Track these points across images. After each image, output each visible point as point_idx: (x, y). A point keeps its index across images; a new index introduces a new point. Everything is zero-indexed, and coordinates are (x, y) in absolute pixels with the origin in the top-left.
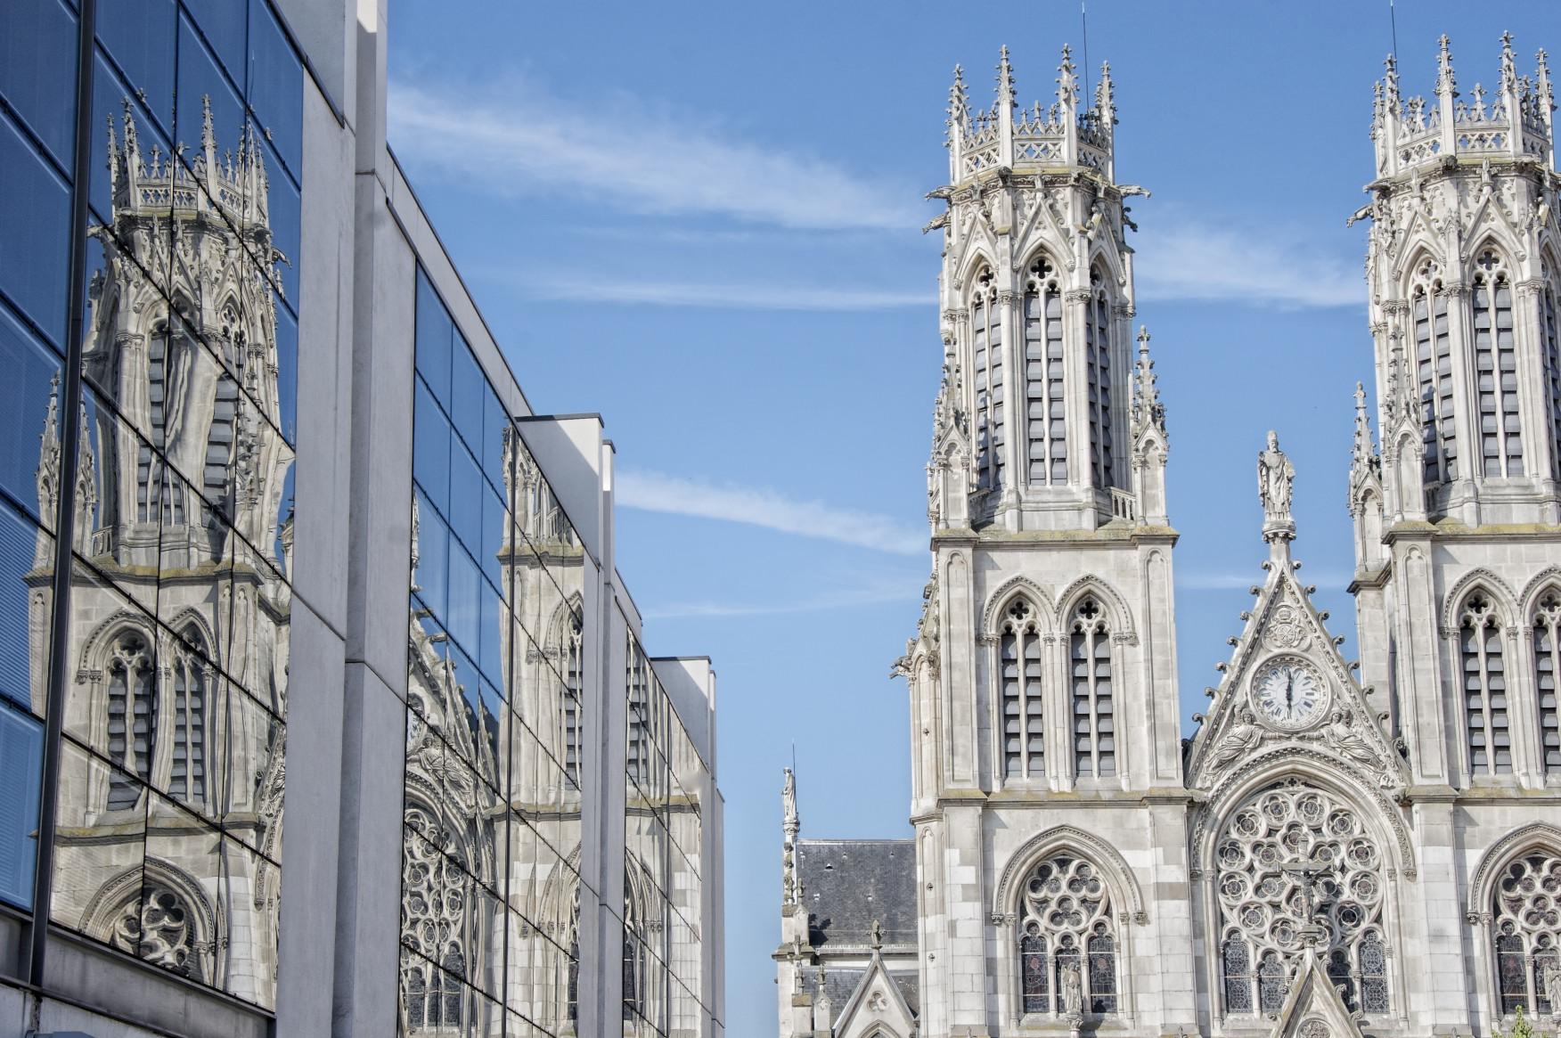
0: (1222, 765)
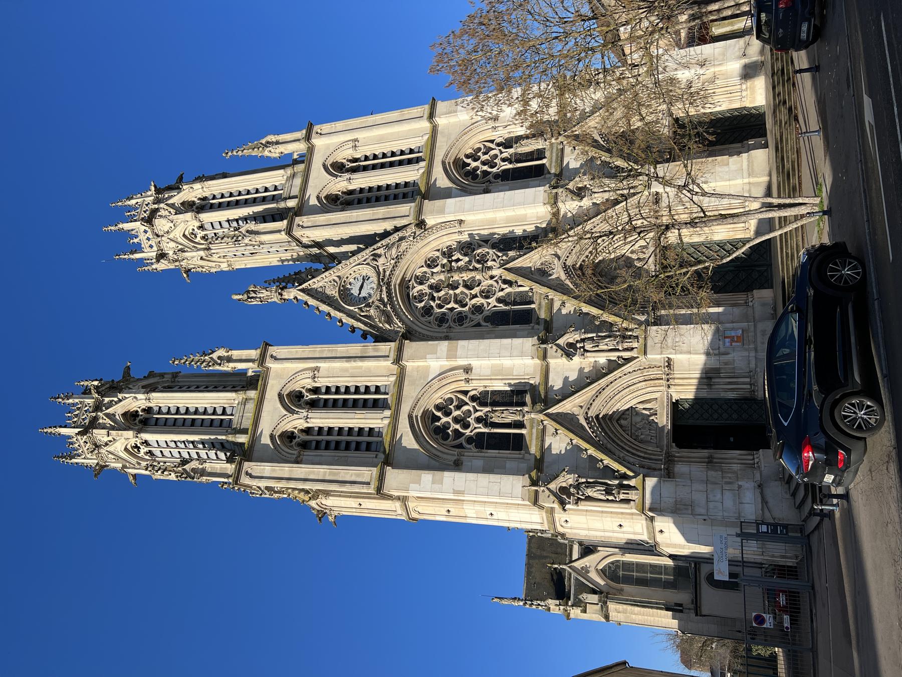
0: (389, 321)
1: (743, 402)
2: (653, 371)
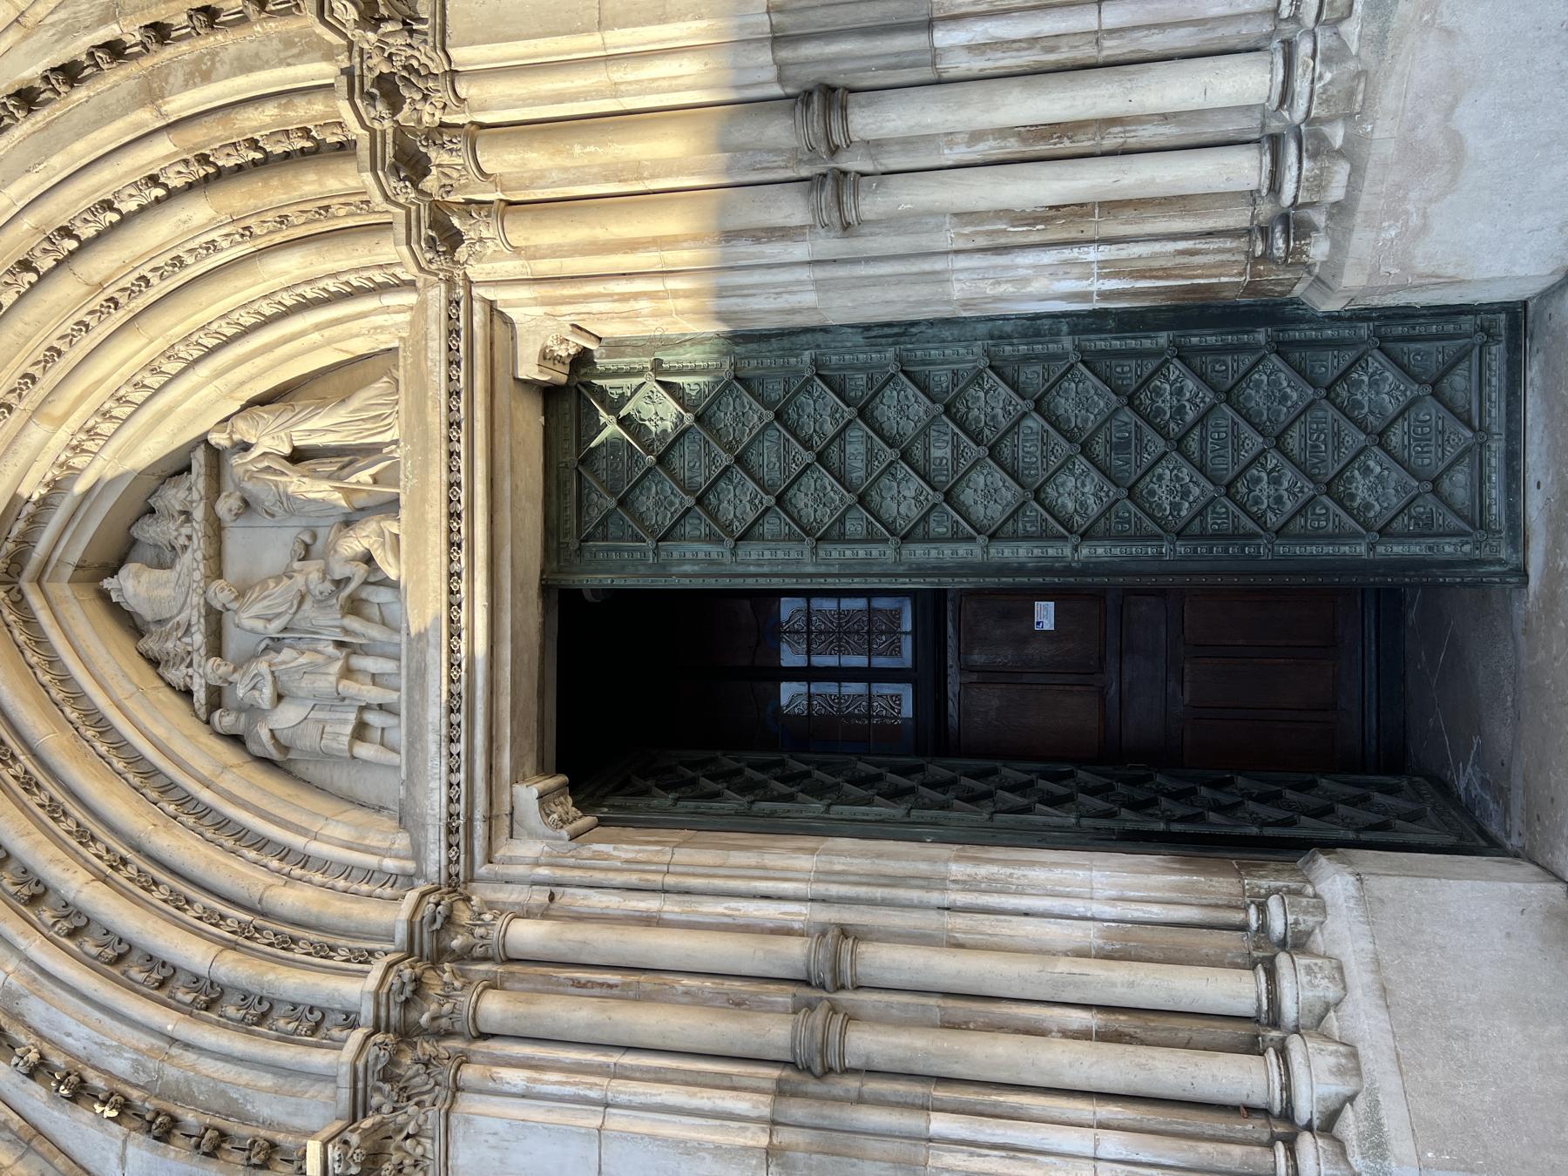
1: (1163, 338)
2: (245, 66)
